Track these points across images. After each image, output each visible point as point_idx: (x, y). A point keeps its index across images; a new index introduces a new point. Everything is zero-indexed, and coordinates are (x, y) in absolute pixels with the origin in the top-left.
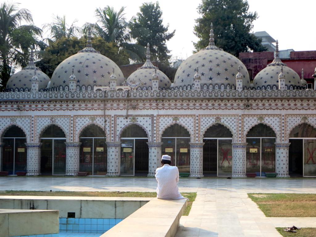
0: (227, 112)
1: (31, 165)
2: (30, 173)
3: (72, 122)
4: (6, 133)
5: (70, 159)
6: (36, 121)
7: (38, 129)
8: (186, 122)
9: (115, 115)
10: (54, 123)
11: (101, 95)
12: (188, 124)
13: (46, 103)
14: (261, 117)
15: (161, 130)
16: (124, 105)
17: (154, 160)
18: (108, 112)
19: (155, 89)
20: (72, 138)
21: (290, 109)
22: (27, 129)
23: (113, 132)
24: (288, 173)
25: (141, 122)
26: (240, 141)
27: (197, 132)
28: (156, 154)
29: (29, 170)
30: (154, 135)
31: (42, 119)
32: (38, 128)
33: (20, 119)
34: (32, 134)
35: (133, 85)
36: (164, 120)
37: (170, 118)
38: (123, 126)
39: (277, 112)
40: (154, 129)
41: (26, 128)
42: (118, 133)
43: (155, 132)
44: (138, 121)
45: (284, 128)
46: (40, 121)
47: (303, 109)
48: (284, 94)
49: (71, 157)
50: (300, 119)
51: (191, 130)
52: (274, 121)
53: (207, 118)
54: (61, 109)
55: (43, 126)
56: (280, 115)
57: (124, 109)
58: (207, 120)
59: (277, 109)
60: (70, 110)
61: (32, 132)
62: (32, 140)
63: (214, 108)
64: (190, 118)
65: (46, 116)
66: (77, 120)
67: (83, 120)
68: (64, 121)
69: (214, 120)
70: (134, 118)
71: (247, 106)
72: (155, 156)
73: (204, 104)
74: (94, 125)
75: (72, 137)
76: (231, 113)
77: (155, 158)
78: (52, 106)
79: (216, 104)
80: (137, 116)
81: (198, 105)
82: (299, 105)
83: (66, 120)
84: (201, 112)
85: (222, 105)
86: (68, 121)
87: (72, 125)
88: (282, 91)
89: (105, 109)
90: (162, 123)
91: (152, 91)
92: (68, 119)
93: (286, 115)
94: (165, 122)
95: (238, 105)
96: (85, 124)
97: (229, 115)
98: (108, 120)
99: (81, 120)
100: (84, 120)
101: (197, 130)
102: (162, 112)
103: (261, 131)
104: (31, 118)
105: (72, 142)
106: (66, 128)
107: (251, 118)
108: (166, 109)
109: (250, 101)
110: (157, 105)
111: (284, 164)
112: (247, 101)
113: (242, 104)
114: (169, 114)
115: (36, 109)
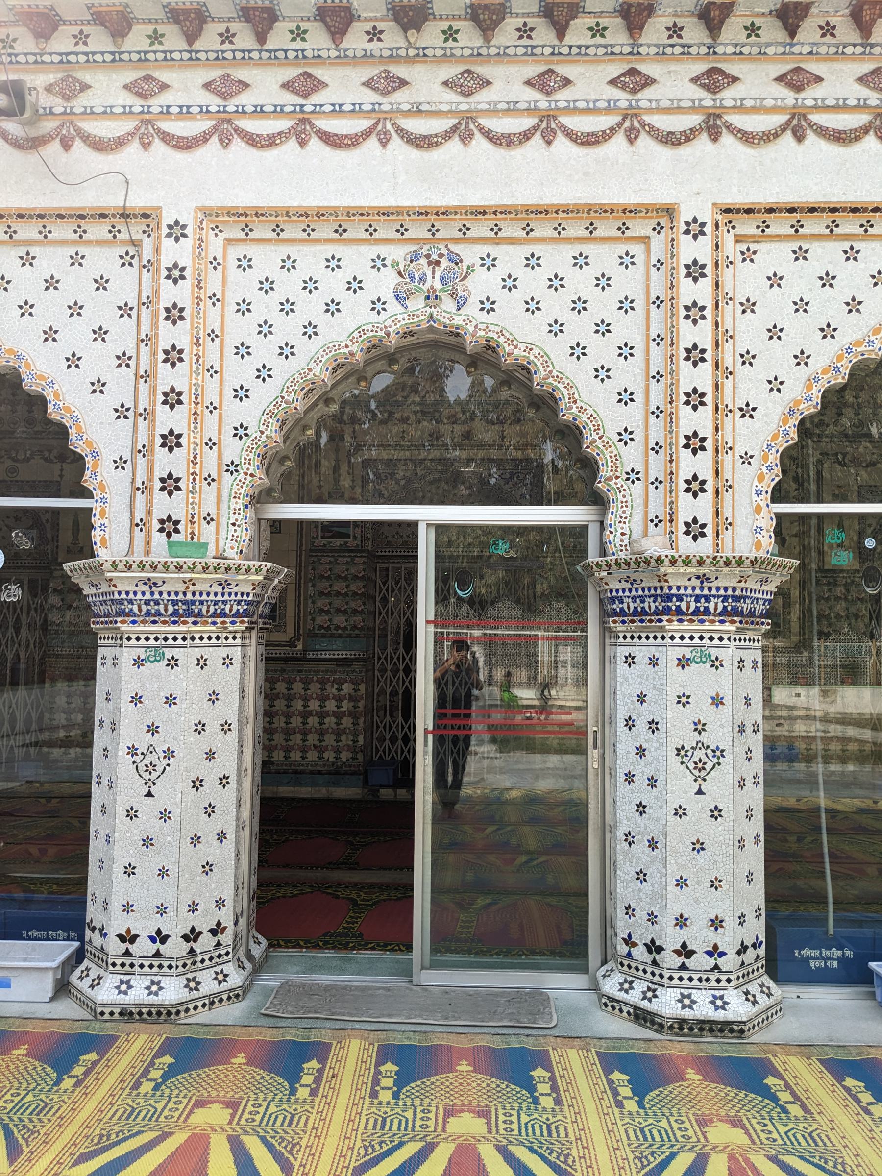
1: (148, 864)
2: (128, 965)
3: (700, 292)
5: (679, 784)
6: (213, 283)
7: (241, 393)
10: (447, 313)
13: (356, 40)
20: (700, 508)
22: (99, 387)
29: (118, 924)
31: (288, 264)
32: (241, 372)
34: (171, 440)
41: (90, 370)
46: (267, 286)
49: (701, 761)
54: (547, 127)
55: (306, 349)
60: (670, 140)
61: (168, 419)
66: (746, 280)
67: (827, 280)
83: (603, 281)
86: (629, 283)
87: (701, 334)
92: (627, 261)
99: (801, 280)
100: (845, 272)
104: (147, 246)
105: (705, 547)
106: (602, 373)
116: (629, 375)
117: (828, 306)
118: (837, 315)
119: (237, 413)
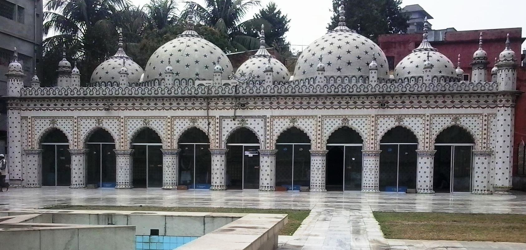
0: (356, 112)
3: (169, 124)
4: (90, 138)
5: (167, 169)
8: (306, 125)
9: (220, 116)
10: (148, 126)
11: (203, 92)
12: (309, 127)
14: (399, 118)
15: (276, 135)
16: (231, 103)
17: (266, 170)
18: (212, 113)
19: (269, 84)
20: (169, 144)
21: (437, 107)
23: (218, 137)
24: (432, 188)
25: (251, 124)
26: (372, 148)
27: (320, 136)
28: (269, 163)
30: (267, 141)
33: (107, 121)
34: (122, 138)
35: (243, 78)
36: (279, 122)
37: (287, 120)
38: (230, 130)
39: (420, 111)
40: (268, 133)
42: (224, 138)
43: (268, 137)
44: (247, 124)
45: (428, 131)
47: (454, 107)
48: (429, 88)
50: (450, 120)
51: (311, 135)
52: (417, 122)
53: (332, 119)
54: (156, 109)
56: (424, 115)
57: (232, 108)
58: (332, 122)
59: (420, 107)
61: (122, 136)
62: (122, 146)
63: (340, 107)
64: (311, 120)
65: (138, 117)
66: (175, 123)
68: (160, 123)
69: (340, 122)
70: (243, 119)
71: (383, 105)
72: (268, 166)
73: (328, 103)
74: (195, 128)
75: (169, 142)
76: (362, 114)
77: (269, 169)
78: (145, 104)
79: (343, 103)
80: (246, 117)
81: (320, 103)
82: (449, 102)
84: (325, 112)
85: (351, 103)
86: (164, 123)
88: (428, 85)
89: (208, 109)
90: (277, 125)
91: (265, 86)
93: (431, 115)
94: (281, 124)
95: (371, 103)
96: (184, 127)
97: (359, 116)
98: (212, 122)
99: (180, 122)
101: (319, 134)
102: (277, 112)
103: (400, 135)
105: (170, 148)
107: (386, 119)
108: (281, 109)
109: (386, 98)
110: (271, 103)
111: (427, 177)
112: (382, 98)
113: (375, 102)
114: (285, 114)
115: (126, 109)
116: (164, 132)
117: (182, 125)
118: (183, 126)
119: (129, 135)
